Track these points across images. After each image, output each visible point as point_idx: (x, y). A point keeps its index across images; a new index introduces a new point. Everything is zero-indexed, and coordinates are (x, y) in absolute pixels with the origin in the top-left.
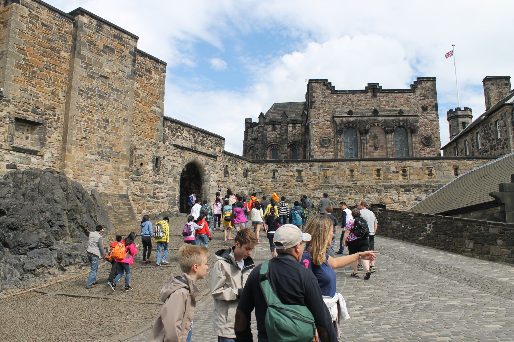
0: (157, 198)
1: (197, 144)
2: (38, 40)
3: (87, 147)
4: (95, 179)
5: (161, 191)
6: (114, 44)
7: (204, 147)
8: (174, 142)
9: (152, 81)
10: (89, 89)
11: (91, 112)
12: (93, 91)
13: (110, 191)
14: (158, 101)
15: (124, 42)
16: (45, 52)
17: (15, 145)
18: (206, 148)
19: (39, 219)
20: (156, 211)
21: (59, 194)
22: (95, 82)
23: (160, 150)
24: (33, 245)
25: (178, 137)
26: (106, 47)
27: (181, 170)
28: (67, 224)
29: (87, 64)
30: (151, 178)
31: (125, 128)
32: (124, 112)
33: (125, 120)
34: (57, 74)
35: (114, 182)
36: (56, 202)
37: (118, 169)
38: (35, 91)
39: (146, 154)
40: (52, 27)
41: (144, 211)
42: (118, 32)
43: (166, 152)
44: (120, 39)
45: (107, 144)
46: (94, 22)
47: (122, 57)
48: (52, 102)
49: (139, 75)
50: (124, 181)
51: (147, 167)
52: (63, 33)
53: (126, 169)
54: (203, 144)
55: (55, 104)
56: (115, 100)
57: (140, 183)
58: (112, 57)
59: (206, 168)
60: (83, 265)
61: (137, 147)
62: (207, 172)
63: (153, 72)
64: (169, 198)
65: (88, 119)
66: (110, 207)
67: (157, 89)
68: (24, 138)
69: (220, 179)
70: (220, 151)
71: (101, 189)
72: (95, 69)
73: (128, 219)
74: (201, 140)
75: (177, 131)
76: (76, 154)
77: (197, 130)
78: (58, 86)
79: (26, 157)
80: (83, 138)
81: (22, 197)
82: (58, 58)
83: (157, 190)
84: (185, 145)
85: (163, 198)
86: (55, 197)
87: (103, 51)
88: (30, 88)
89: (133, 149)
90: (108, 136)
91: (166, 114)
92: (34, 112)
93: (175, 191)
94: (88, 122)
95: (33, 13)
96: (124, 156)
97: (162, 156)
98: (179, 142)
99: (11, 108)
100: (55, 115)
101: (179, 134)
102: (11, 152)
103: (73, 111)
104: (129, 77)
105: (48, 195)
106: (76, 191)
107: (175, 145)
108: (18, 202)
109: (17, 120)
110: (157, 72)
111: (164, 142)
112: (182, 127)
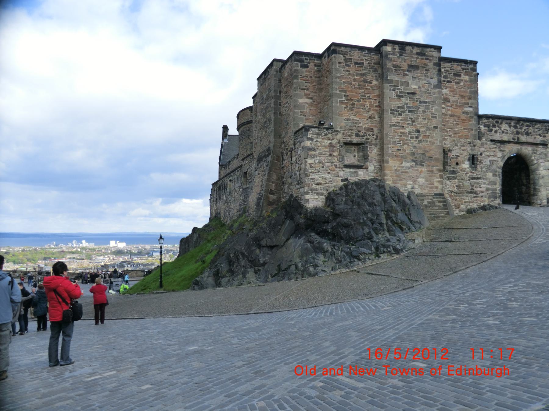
0: (475, 193)
1: (520, 136)
2: (353, 78)
3: (402, 157)
4: (412, 183)
5: (480, 186)
6: (419, 61)
7: (529, 136)
9: (462, 84)
10: (399, 107)
11: (403, 127)
12: (403, 108)
13: (426, 191)
14: (470, 101)
15: (427, 56)
16: (359, 85)
17: (346, 163)
18: (533, 137)
19: (363, 219)
20: (475, 205)
21: (378, 198)
22: (403, 100)
23: (476, 147)
24: (360, 238)
25: (496, 132)
26: (410, 66)
27: (502, 164)
28: (384, 221)
29: (395, 86)
30: (468, 175)
31: (436, 135)
32: (434, 120)
33: (436, 127)
34: (372, 100)
35: (429, 182)
36: (375, 205)
37: (432, 171)
38: (356, 119)
39: (460, 153)
40: (363, 63)
41: (462, 206)
42: (421, 49)
43: (482, 149)
44: (423, 54)
45: (420, 151)
46: (397, 47)
47: (426, 70)
48: (370, 124)
49: (448, 82)
50: (439, 181)
51: (464, 165)
52: (373, 65)
53: (440, 171)
54: (527, 134)
55: (373, 126)
56: (424, 111)
57: (456, 180)
58: (417, 73)
59: (533, 158)
60: (393, 253)
61: (451, 149)
62: (535, 162)
63: (462, 74)
64: (490, 192)
65: (401, 133)
66: (426, 206)
67: (468, 90)
68: (352, 157)
71: (418, 190)
72: (402, 88)
73: (442, 215)
74: (525, 130)
75: (494, 126)
76: (392, 164)
77: (519, 120)
78: (373, 110)
79: (355, 172)
80: (398, 149)
81: (351, 203)
82: (371, 87)
83: (475, 185)
84: (506, 138)
85: (482, 192)
86: (375, 201)
87: (408, 71)
88: (352, 117)
89: (445, 152)
90: (421, 144)
91: (481, 112)
92: (357, 135)
93: (495, 184)
94: (401, 136)
95: (347, 57)
96: (437, 160)
97: (479, 153)
98: (497, 137)
99: (340, 136)
100: (373, 135)
101: (497, 128)
102: (344, 169)
103: (387, 128)
104: (436, 87)
105: (370, 200)
106: (392, 195)
107: (492, 141)
108: (349, 207)
109: (346, 144)
110: (466, 74)
111: (480, 138)
112: (500, 121)
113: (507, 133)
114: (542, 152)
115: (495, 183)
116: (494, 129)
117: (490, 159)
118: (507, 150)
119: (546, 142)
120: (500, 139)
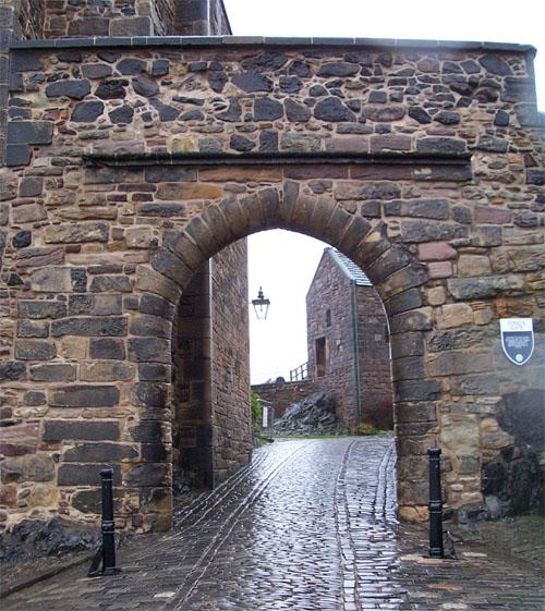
7: (346, 125)
8: (89, 149)
25: (124, 116)
54: (332, 113)
59: (376, 237)
64: (66, 447)
74: (316, 92)
84: (186, 140)
98: (135, 137)
101: (132, 98)
107: (94, 162)
114: (435, 204)
115: (109, 398)
116: (109, 107)
117: (82, 259)
118: (192, 207)
120: (148, 150)
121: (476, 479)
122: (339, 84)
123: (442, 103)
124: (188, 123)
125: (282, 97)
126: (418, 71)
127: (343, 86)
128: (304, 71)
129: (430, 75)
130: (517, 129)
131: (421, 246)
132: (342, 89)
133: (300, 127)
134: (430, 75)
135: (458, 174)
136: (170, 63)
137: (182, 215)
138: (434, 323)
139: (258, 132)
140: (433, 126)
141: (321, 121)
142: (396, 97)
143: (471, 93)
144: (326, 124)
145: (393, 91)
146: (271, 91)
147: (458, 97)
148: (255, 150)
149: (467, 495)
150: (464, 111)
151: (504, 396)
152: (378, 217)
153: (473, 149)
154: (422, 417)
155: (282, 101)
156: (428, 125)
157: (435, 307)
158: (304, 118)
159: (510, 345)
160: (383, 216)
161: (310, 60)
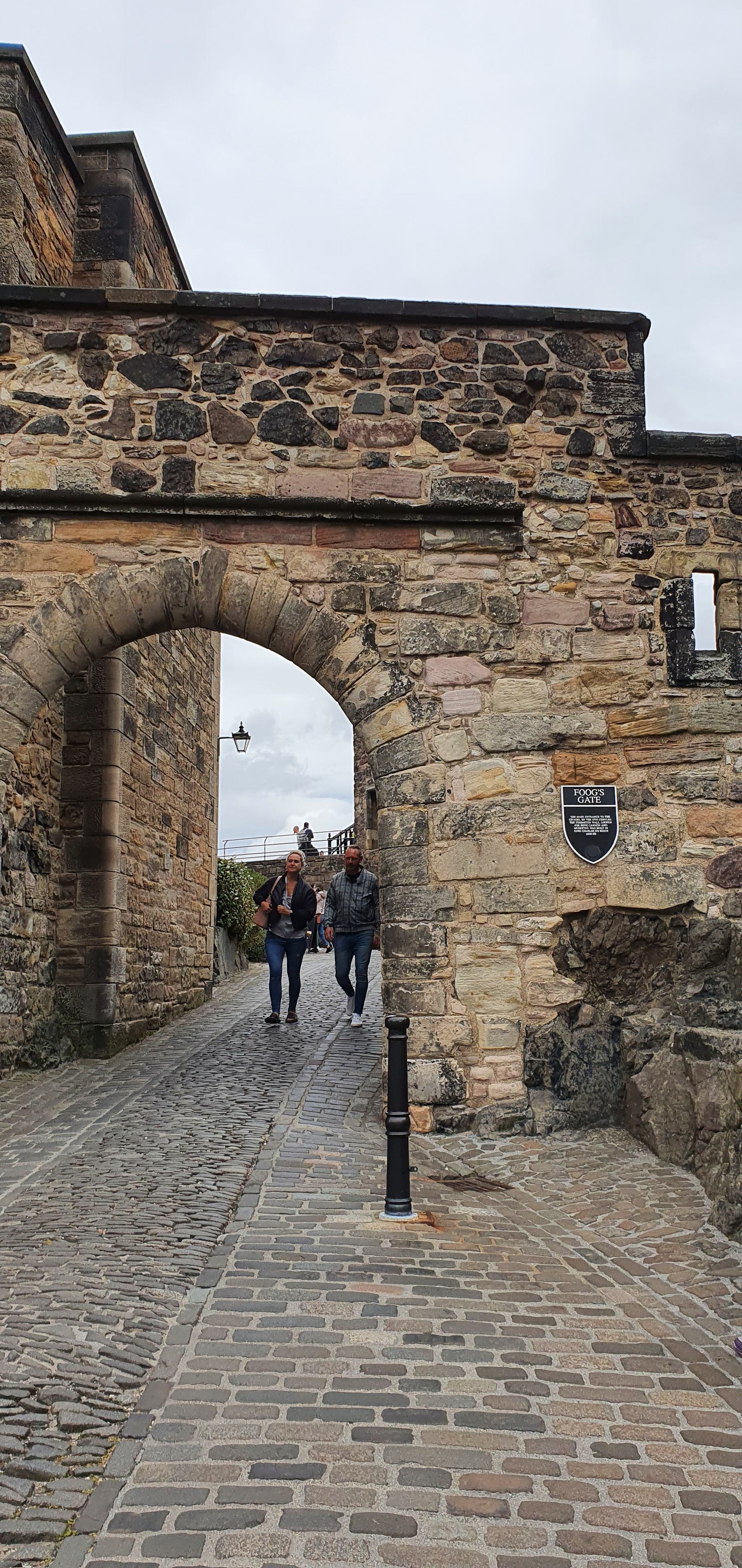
1: (200, 447)
7: (313, 453)
18: (354, 454)
54: (291, 429)
69: (596, 723)
70: (581, 447)
74: (262, 392)
113: (60, 427)
114: (457, 590)
119: (504, 490)
121: (513, 1060)
122: (304, 379)
123: (479, 416)
124: (39, 438)
125: (206, 399)
126: (440, 359)
127: (312, 383)
128: (241, 356)
129: (461, 366)
130: (606, 462)
131: (430, 661)
132: (309, 388)
133: (231, 454)
134: (461, 366)
135: (497, 537)
136: (14, 333)
137: (23, 598)
138: (446, 791)
139: (163, 459)
140: (462, 456)
141: (270, 444)
142: (401, 403)
143: (531, 399)
144: (278, 448)
145: (395, 394)
146: (186, 389)
147: (507, 405)
148: (155, 489)
149: (497, 1088)
150: (516, 428)
151: (569, 917)
152: (359, 612)
153: (527, 497)
154: (422, 948)
155: (204, 406)
156: (452, 455)
157: (450, 764)
158: (240, 438)
159: (577, 830)
160: (369, 608)
161: (256, 336)
